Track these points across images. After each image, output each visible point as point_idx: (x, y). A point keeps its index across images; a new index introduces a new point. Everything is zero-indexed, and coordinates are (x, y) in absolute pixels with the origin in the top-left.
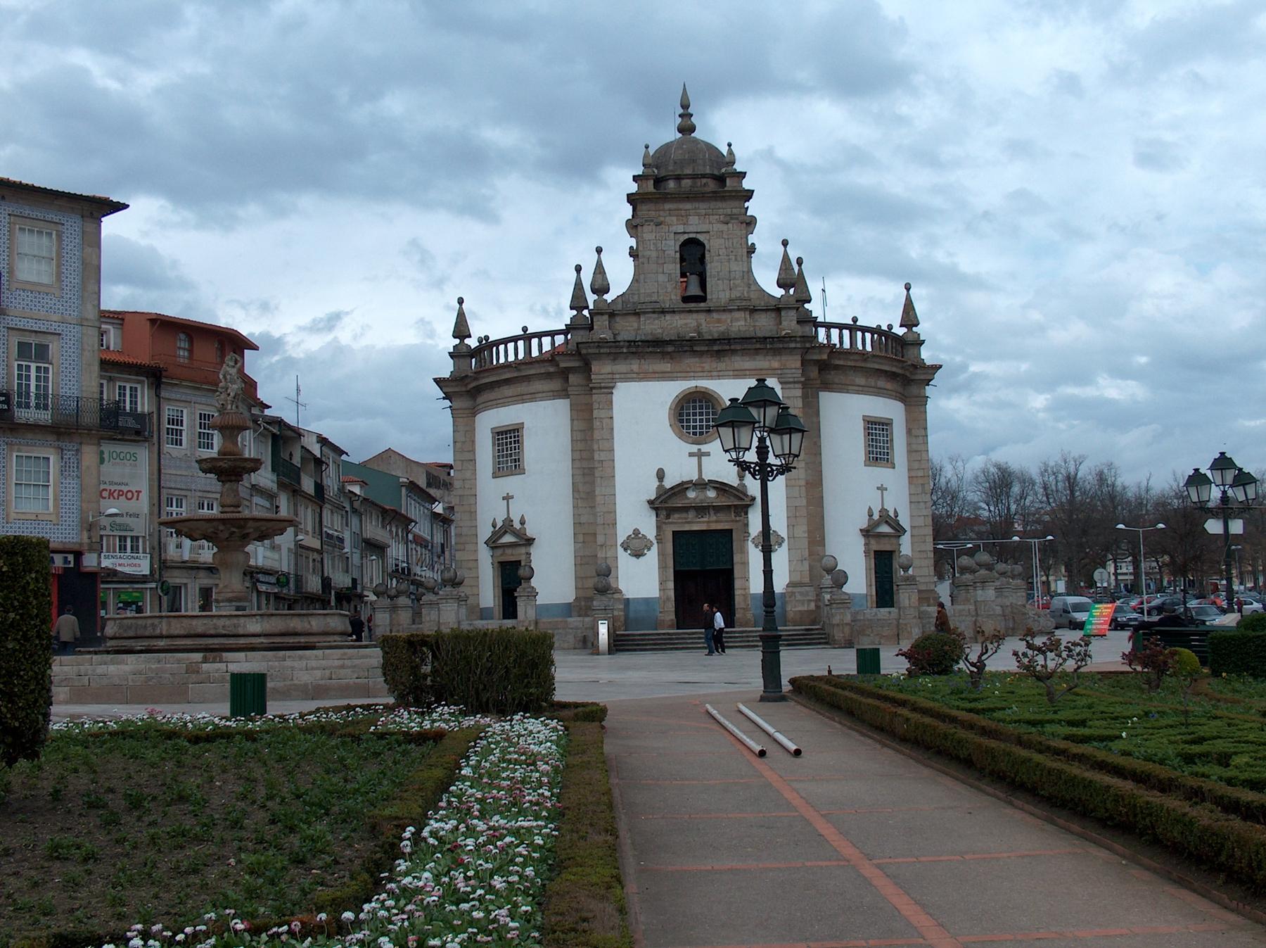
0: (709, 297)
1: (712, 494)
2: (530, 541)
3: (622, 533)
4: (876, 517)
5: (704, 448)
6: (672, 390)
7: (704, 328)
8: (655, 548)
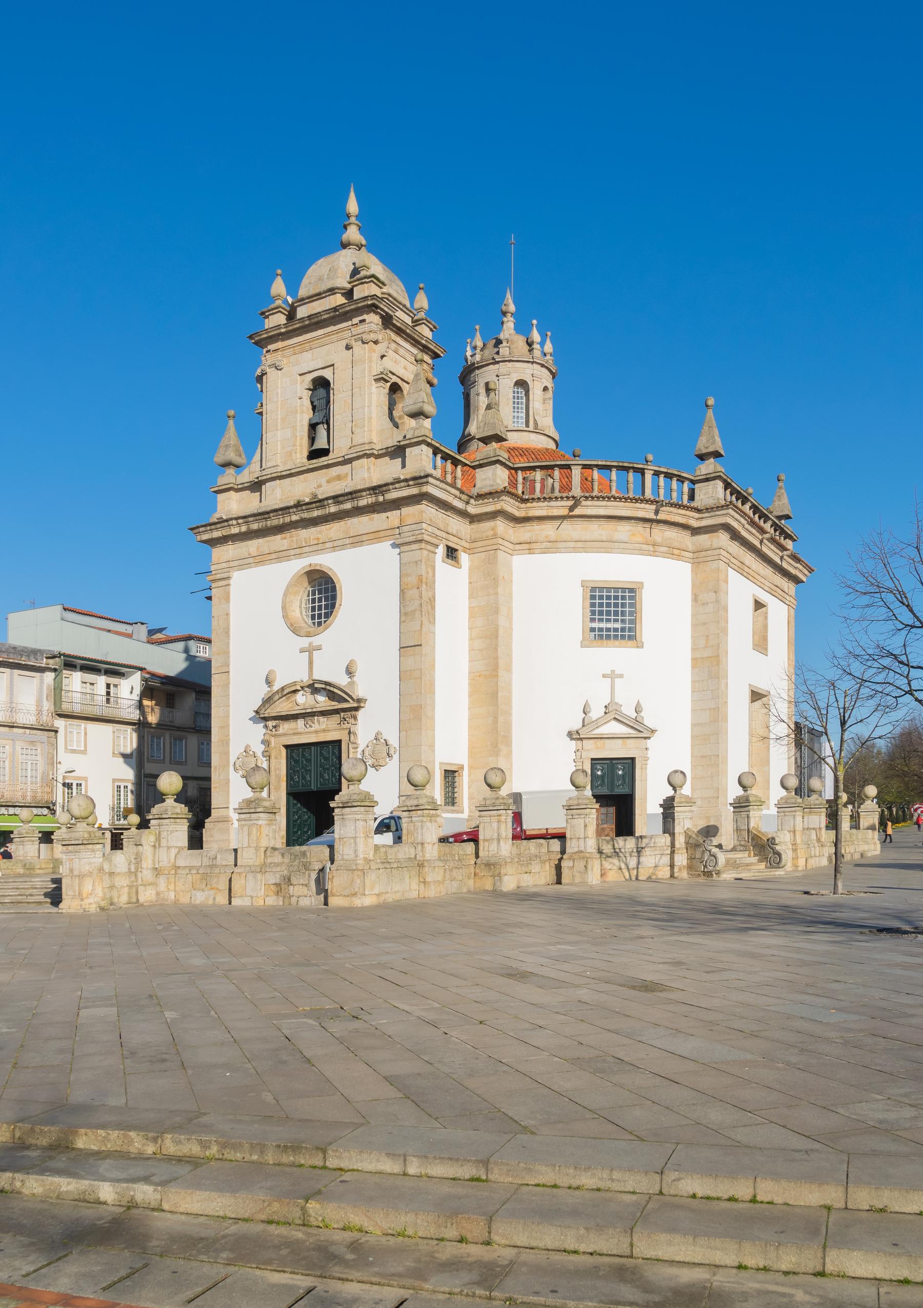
4: (597, 712)
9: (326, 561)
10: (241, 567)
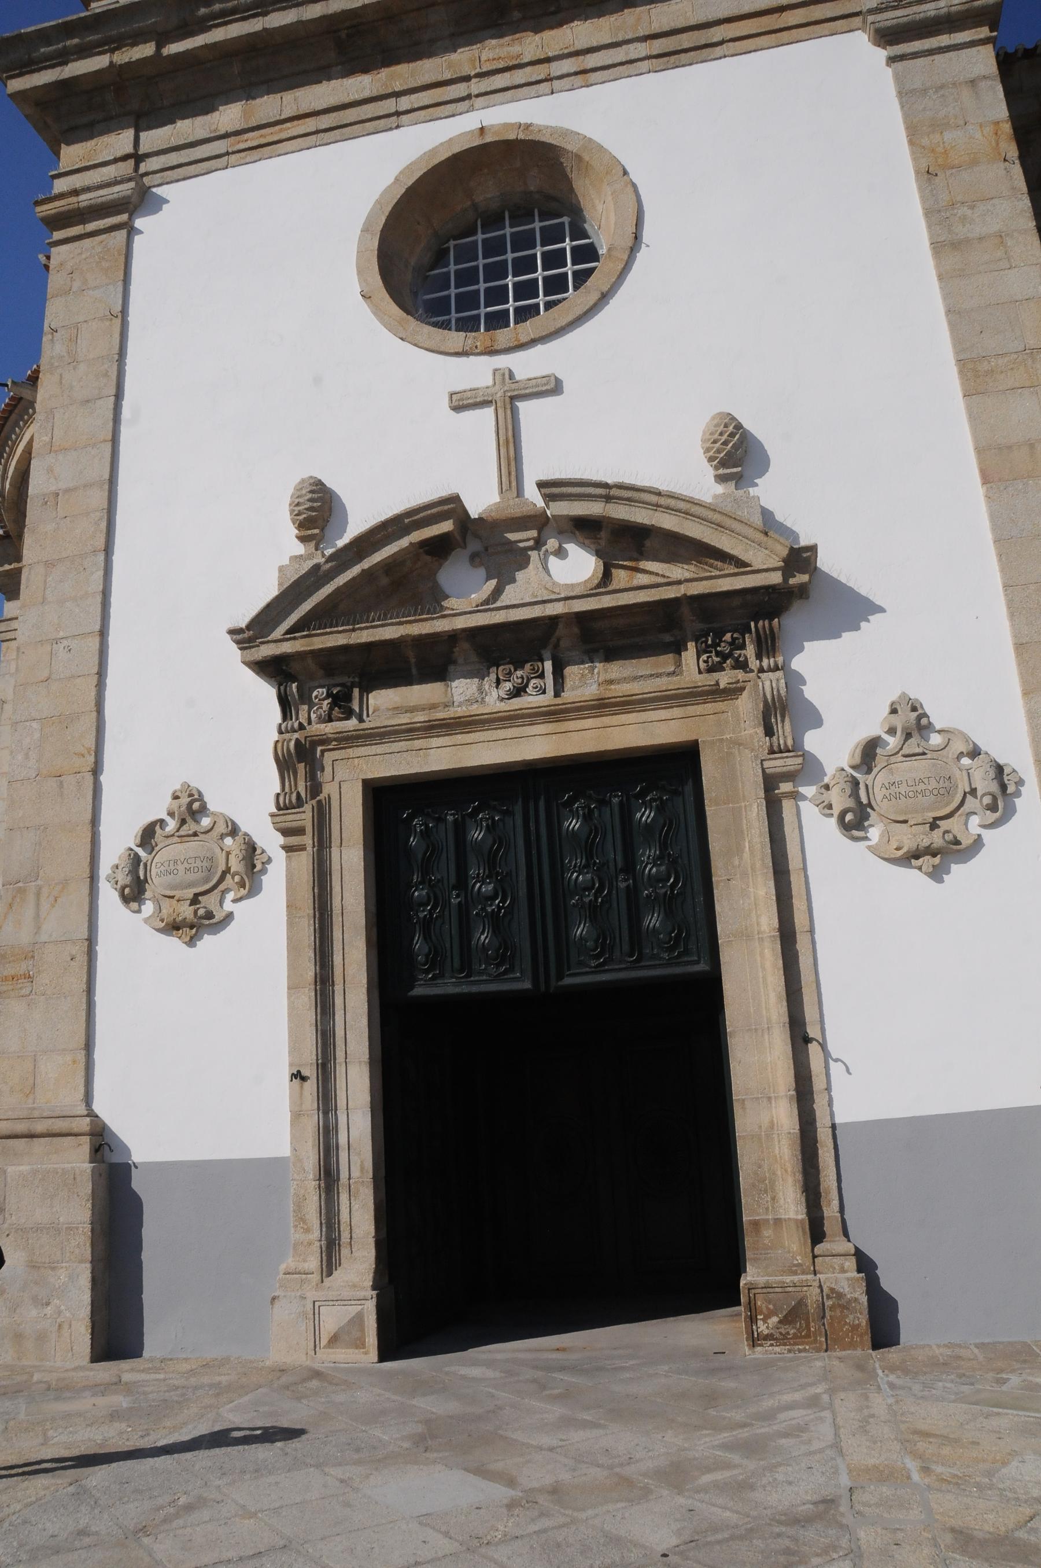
1: (575, 567)
5: (526, 365)
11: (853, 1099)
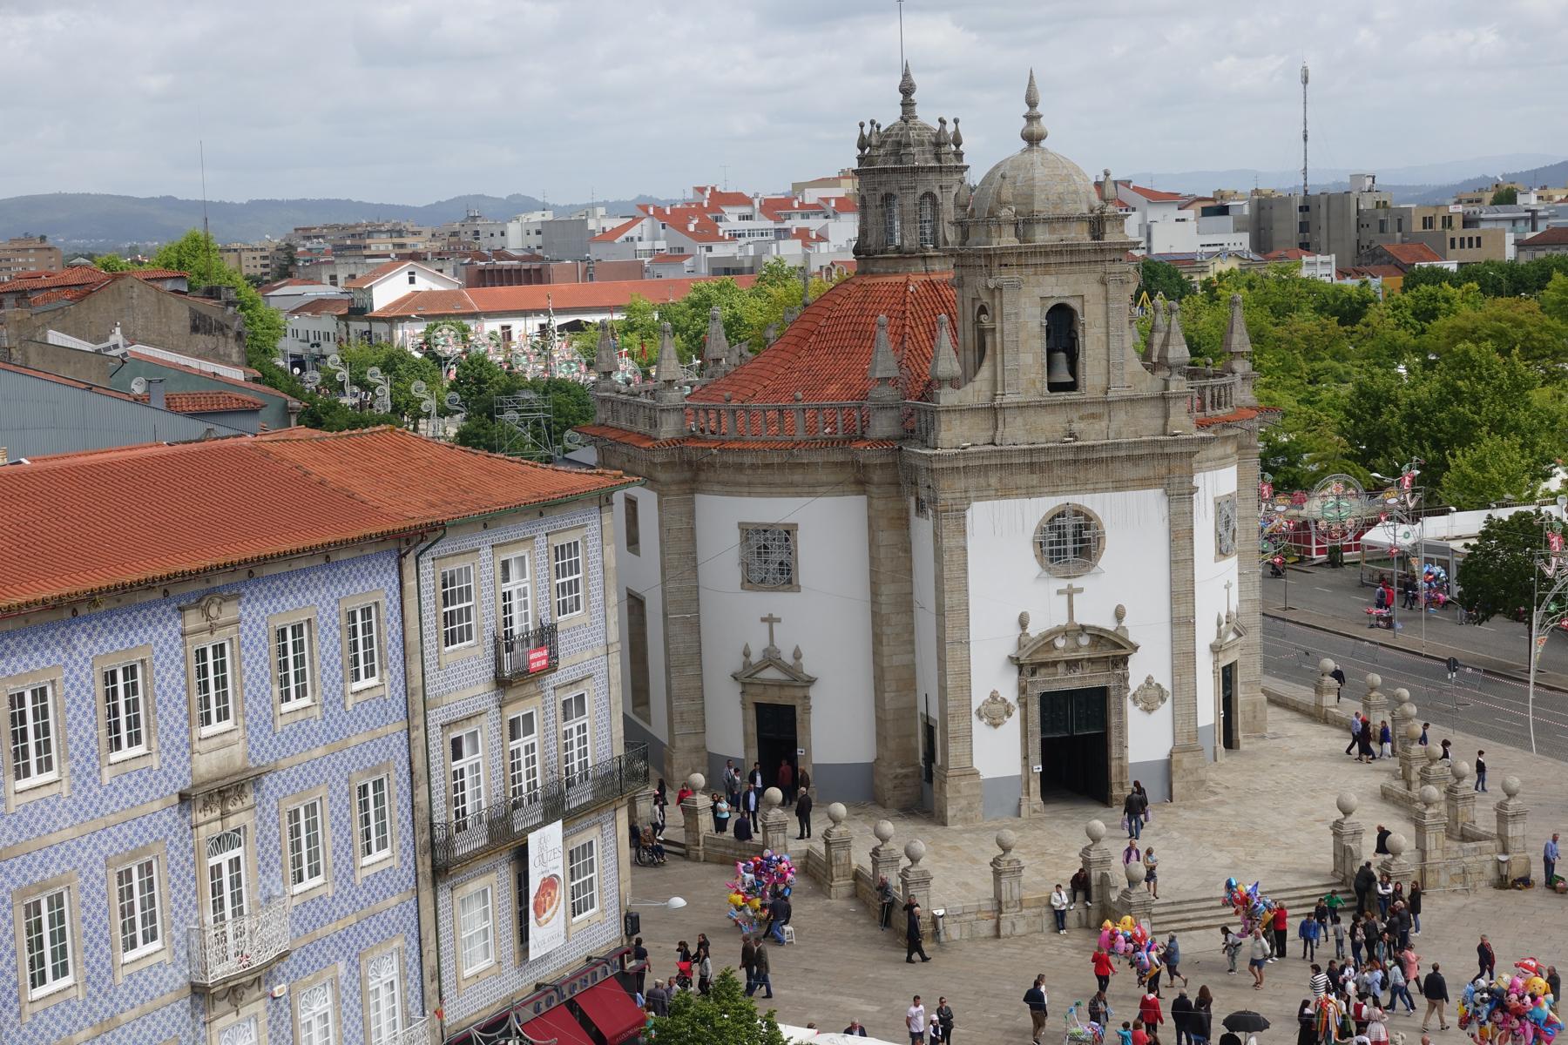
0: (1081, 383)
1: (1084, 641)
2: (811, 681)
3: (979, 698)
5: (1076, 583)
6: (1035, 510)
7: (1076, 427)
8: (1017, 713)
9: (1087, 501)
10: (978, 499)
11: (1131, 760)
